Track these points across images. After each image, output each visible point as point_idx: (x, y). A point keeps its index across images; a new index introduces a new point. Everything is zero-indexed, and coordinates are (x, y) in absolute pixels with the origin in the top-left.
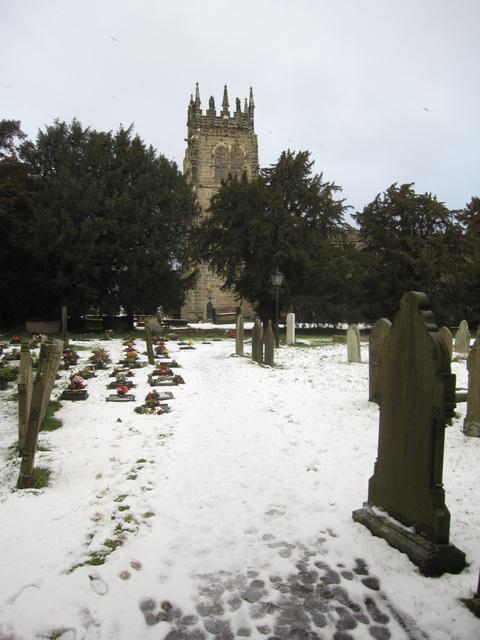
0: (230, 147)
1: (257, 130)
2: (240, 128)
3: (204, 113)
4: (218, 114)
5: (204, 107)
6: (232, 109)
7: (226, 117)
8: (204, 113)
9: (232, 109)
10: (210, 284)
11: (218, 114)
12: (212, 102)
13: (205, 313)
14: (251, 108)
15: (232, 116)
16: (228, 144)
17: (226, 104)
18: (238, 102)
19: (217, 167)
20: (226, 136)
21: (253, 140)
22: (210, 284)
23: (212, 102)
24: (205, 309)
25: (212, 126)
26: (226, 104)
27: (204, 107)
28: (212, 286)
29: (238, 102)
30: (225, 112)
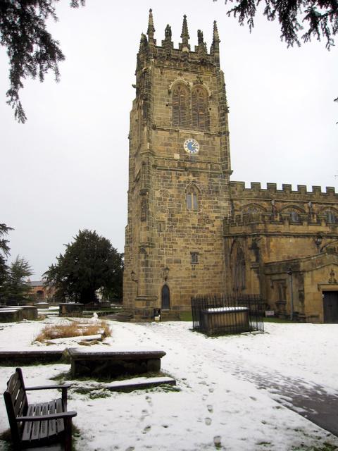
0: (191, 84)
1: (223, 66)
2: (204, 63)
3: (159, 44)
4: (176, 46)
5: (159, 37)
6: (193, 42)
7: (185, 49)
8: (159, 44)
9: (193, 42)
10: (165, 258)
11: (176, 46)
12: (168, 32)
13: (159, 300)
14: (216, 42)
15: (193, 49)
16: (189, 79)
17: (185, 35)
18: (200, 35)
19: (175, 108)
20: (186, 70)
21: (219, 76)
22: (165, 258)
23: (168, 32)
24: (159, 295)
25: (169, 57)
26: (185, 35)
27: (159, 37)
28: (168, 261)
29: (200, 35)
30: (185, 43)
